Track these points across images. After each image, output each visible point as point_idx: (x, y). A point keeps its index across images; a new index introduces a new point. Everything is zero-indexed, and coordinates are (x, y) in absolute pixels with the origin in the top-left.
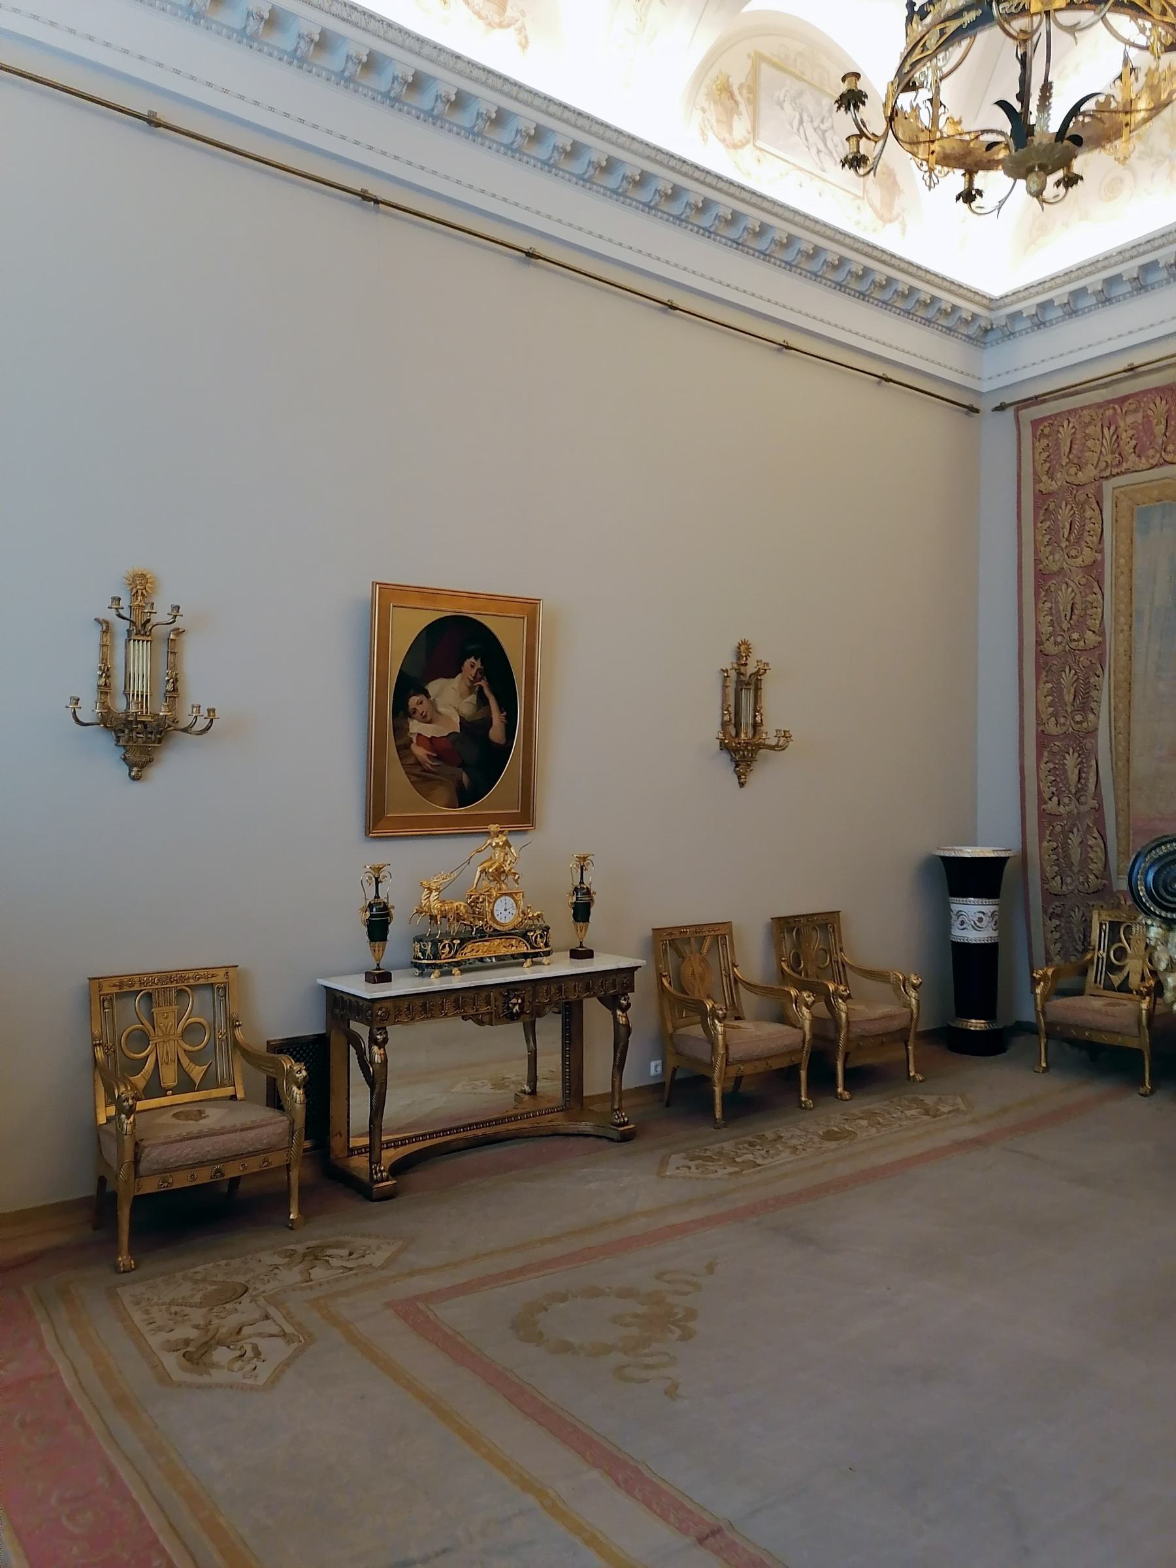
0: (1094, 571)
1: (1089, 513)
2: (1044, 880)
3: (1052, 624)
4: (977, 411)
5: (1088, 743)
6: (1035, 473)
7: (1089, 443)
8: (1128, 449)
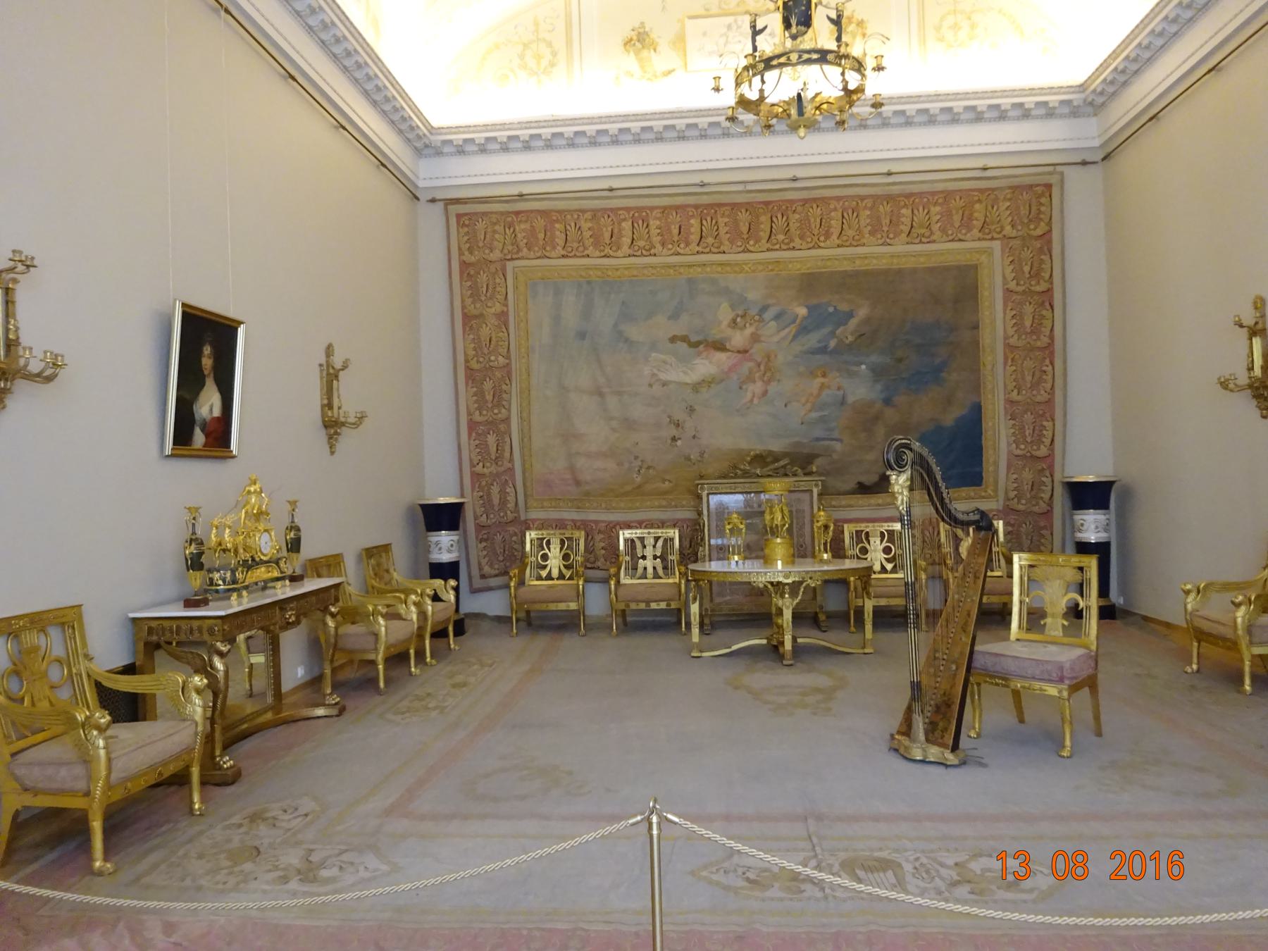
0: (503, 317)
1: (498, 280)
2: (476, 518)
3: (475, 349)
4: (417, 199)
5: (502, 427)
6: (460, 249)
7: (497, 236)
8: (522, 244)
